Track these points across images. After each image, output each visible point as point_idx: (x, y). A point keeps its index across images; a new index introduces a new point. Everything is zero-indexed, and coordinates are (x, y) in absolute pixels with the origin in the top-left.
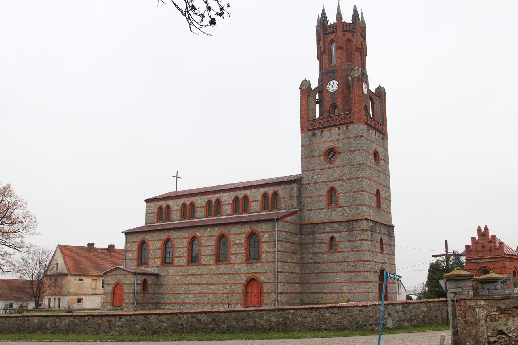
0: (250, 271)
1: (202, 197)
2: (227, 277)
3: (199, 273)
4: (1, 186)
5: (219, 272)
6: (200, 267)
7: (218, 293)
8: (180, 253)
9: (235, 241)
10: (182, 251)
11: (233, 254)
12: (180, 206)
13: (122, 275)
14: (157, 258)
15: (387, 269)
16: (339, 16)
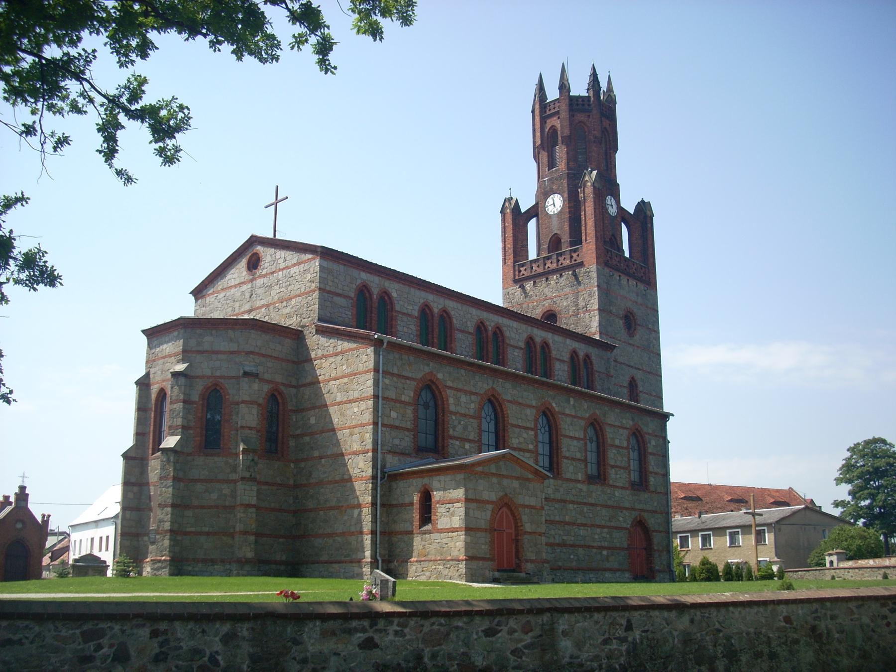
0: (638, 506)
1: (465, 307)
2: (604, 512)
3: (558, 496)
4: (419, 12)
5: (593, 501)
6: (560, 482)
7: (593, 547)
8: (521, 440)
9: (613, 439)
10: (525, 435)
11: (613, 467)
12: (417, 308)
13: (517, 478)
14: (469, 441)
15: (652, 522)
16: (564, 87)
